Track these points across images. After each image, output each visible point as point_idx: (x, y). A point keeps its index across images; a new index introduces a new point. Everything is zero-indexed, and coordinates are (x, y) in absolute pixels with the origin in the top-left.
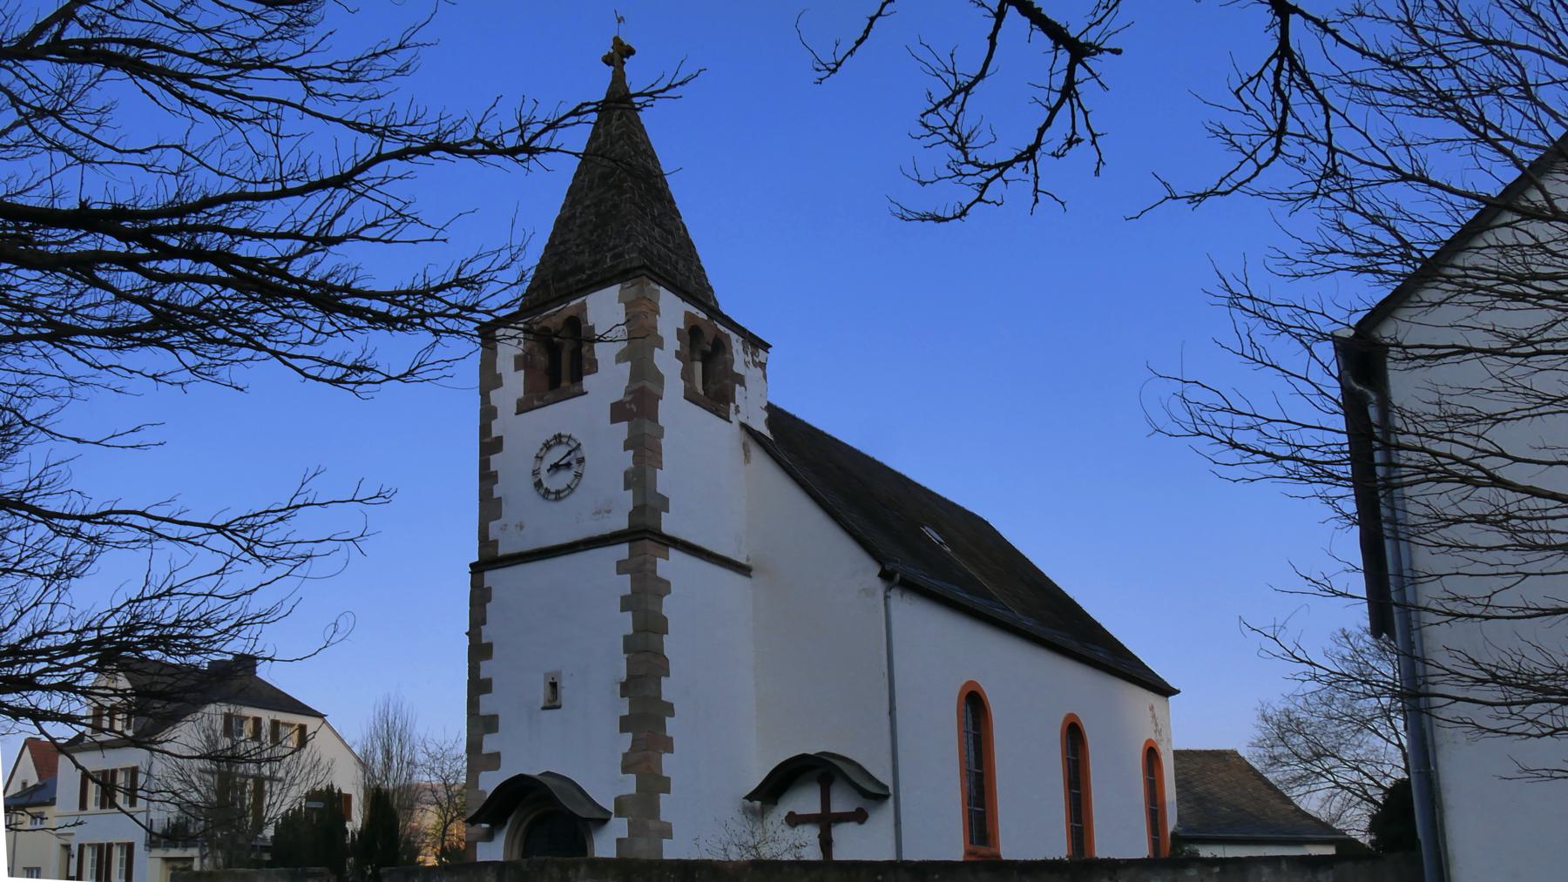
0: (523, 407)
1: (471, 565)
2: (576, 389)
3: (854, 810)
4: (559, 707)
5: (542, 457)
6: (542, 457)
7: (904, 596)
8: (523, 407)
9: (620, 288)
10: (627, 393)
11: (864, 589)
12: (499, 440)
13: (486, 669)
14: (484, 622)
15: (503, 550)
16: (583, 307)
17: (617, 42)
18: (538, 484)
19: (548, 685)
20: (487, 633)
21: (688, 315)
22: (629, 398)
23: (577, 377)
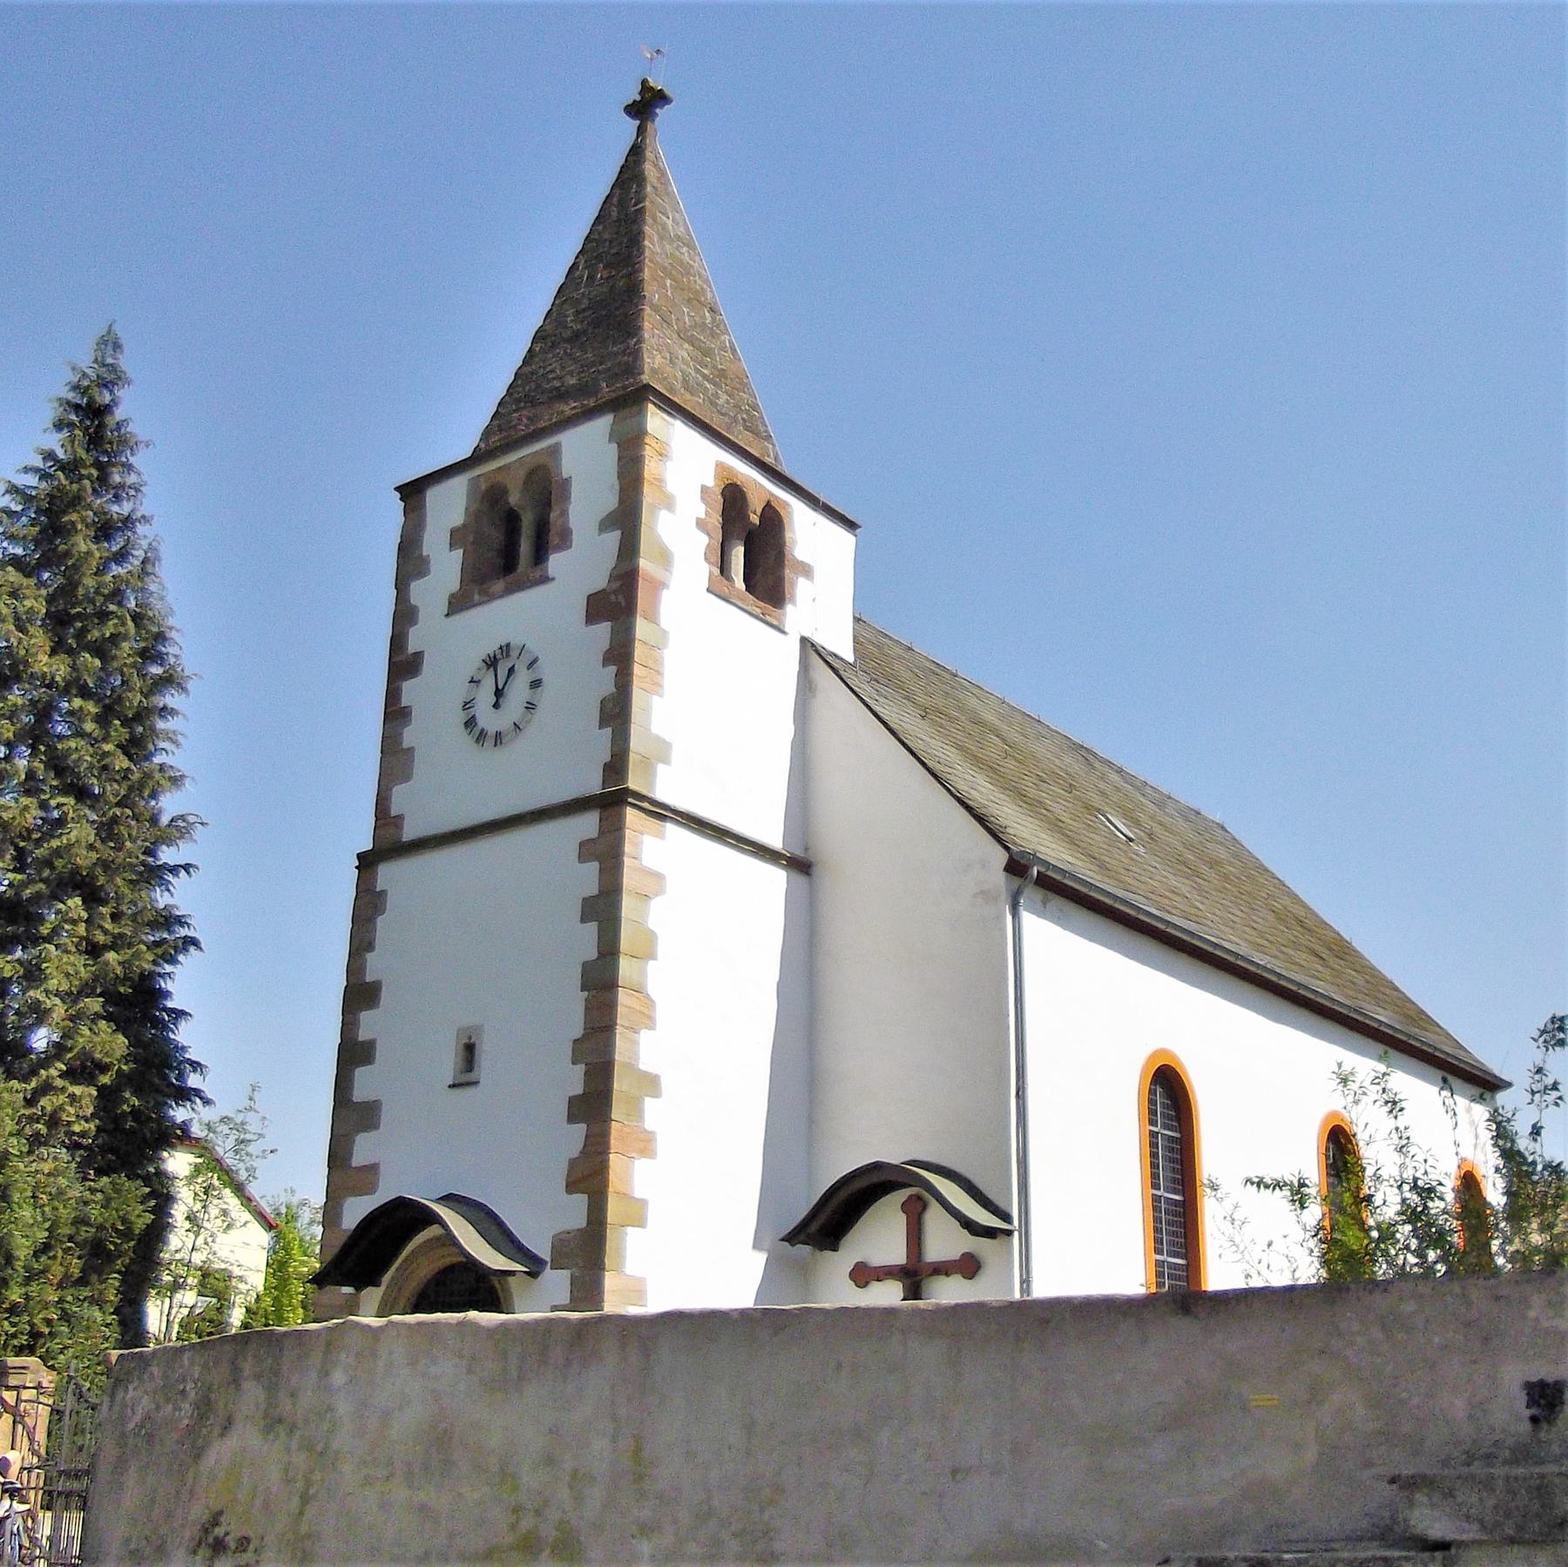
0: (458, 604)
1: (359, 856)
2: (538, 574)
3: (904, 1216)
4: (476, 1083)
5: (479, 681)
6: (479, 681)
7: (1048, 905)
8: (458, 604)
9: (612, 421)
10: (612, 578)
11: (982, 892)
12: (419, 656)
13: (370, 1024)
14: (370, 946)
15: (409, 833)
16: (555, 451)
17: (645, 86)
18: (470, 723)
19: (461, 1047)
20: (375, 965)
21: (720, 466)
22: (615, 586)
23: (540, 554)
